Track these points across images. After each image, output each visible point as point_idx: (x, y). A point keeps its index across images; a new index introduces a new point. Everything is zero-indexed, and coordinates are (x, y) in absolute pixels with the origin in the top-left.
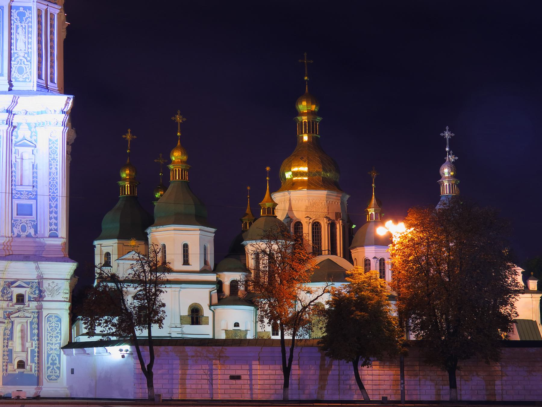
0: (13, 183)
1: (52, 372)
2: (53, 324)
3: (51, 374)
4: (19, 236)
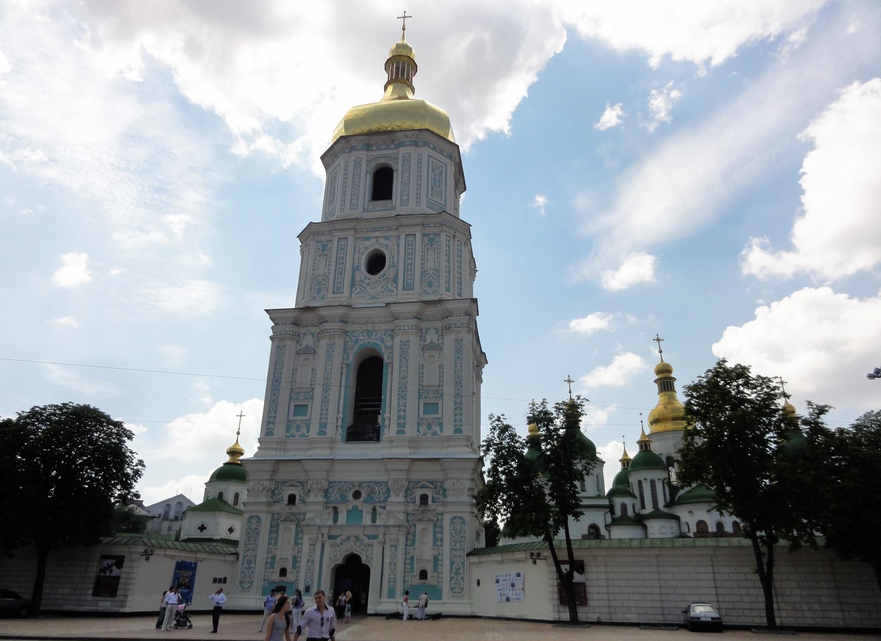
0: (421, 383)
1: (456, 583)
2: (458, 527)
4: (425, 434)
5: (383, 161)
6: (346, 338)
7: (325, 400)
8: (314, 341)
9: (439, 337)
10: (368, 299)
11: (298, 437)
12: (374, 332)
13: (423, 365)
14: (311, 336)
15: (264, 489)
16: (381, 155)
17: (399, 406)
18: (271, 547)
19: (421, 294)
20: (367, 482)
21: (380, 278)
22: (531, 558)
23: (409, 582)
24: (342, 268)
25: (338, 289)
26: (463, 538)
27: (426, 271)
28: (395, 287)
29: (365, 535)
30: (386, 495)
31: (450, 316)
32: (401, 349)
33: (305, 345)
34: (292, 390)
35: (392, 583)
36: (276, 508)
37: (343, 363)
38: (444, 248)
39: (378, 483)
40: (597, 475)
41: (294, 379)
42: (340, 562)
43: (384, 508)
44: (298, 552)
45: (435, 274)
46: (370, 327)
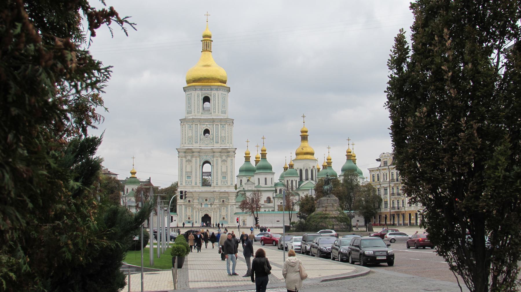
4: (223, 185)
5: (206, 95)
7: (196, 175)
16: (206, 93)
25: (196, 141)
34: (186, 172)
38: (227, 129)
39: (212, 197)
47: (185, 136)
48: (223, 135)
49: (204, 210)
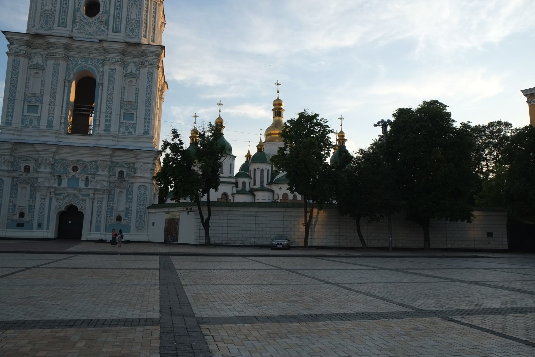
0: (122, 99)
1: (140, 224)
3: (138, 225)
4: (123, 133)
6: (68, 62)
7: (52, 104)
8: (43, 60)
9: (136, 69)
10: (86, 35)
11: (31, 127)
12: (90, 60)
13: (124, 87)
14: (40, 56)
15: (5, 161)
17: (106, 113)
18: (12, 199)
19: (125, 37)
20: (82, 161)
21: (95, 20)
22: (187, 211)
23: (110, 222)
24: (65, 8)
26: (146, 198)
27: (130, 20)
28: (106, 29)
29: (80, 194)
30: (95, 170)
31: (146, 56)
32: (109, 74)
33: (36, 63)
34: (25, 94)
35: (98, 223)
36: (15, 174)
37: (65, 79)
39: (90, 162)
40: (231, 164)
41: (27, 87)
42: (63, 210)
43: (94, 178)
44: (33, 203)
45: (136, 24)
46: (87, 55)
47: (36, 9)
48: (133, 16)
49: (66, 194)
